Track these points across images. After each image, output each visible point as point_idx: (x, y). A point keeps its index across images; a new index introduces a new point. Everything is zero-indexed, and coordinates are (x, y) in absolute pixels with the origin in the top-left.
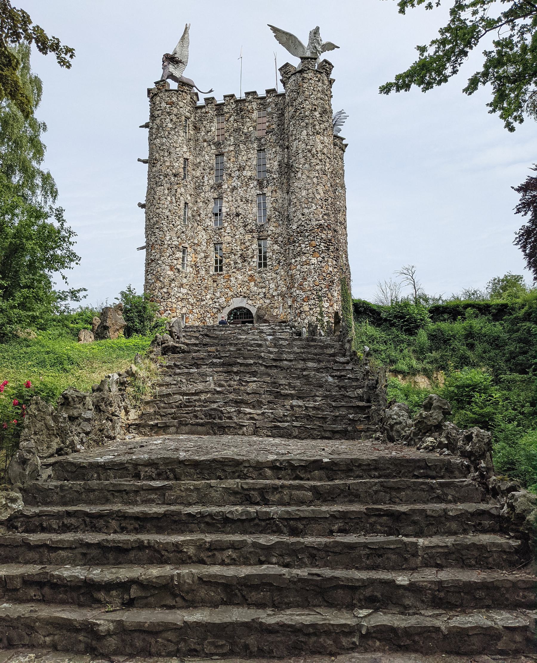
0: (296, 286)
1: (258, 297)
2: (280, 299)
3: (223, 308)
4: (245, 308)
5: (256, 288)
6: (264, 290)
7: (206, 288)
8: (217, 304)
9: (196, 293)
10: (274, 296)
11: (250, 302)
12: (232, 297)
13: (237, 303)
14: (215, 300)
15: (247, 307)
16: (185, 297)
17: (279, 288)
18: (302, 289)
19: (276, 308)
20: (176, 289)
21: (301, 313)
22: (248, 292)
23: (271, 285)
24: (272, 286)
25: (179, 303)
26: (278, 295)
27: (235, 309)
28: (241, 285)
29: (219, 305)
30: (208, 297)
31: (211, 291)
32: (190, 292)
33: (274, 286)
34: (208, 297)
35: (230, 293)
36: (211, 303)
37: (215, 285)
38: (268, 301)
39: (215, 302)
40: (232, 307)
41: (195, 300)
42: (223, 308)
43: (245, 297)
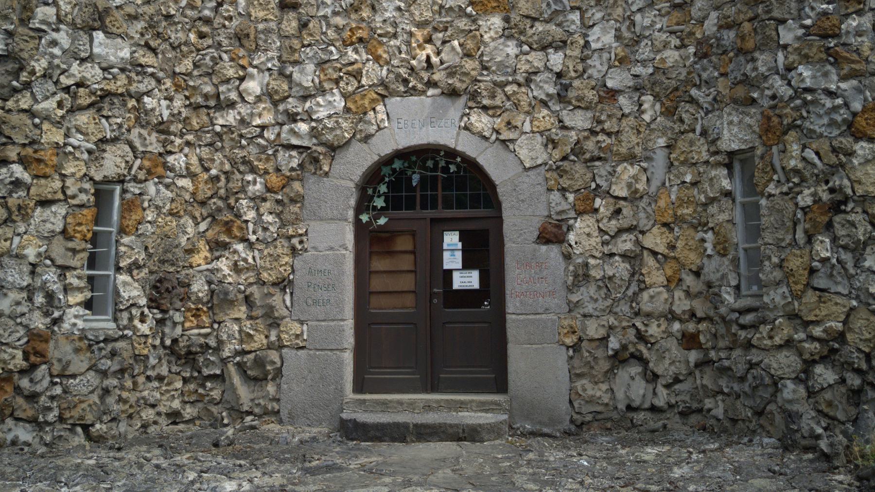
0: (788, 35)
1: (525, 97)
2: (650, 108)
3: (333, 149)
4: (451, 154)
5: (512, 49)
6: (556, 59)
7: (240, 37)
8: (303, 127)
9: (186, 65)
10: (613, 94)
11: (481, 121)
12: (384, 91)
13: (410, 124)
14: (292, 104)
15: (467, 146)
16: (120, 85)
17: (644, 51)
18: (837, 61)
19: (631, 158)
20: (63, 37)
21: (837, 207)
22: (470, 65)
23: (595, 34)
24: (602, 37)
25: (83, 119)
26: (638, 89)
27: (401, 154)
28: (433, 30)
29: (314, 133)
30: (253, 86)
31: (268, 58)
32: (148, 59)
33: (608, 39)
34: (253, 86)
35: (373, 73)
36: (268, 118)
37: (291, 24)
38: (579, 120)
39: (293, 118)
40: (386, 144)
41: (178, 103)
42: (333, 149)
43: (453, 93)
